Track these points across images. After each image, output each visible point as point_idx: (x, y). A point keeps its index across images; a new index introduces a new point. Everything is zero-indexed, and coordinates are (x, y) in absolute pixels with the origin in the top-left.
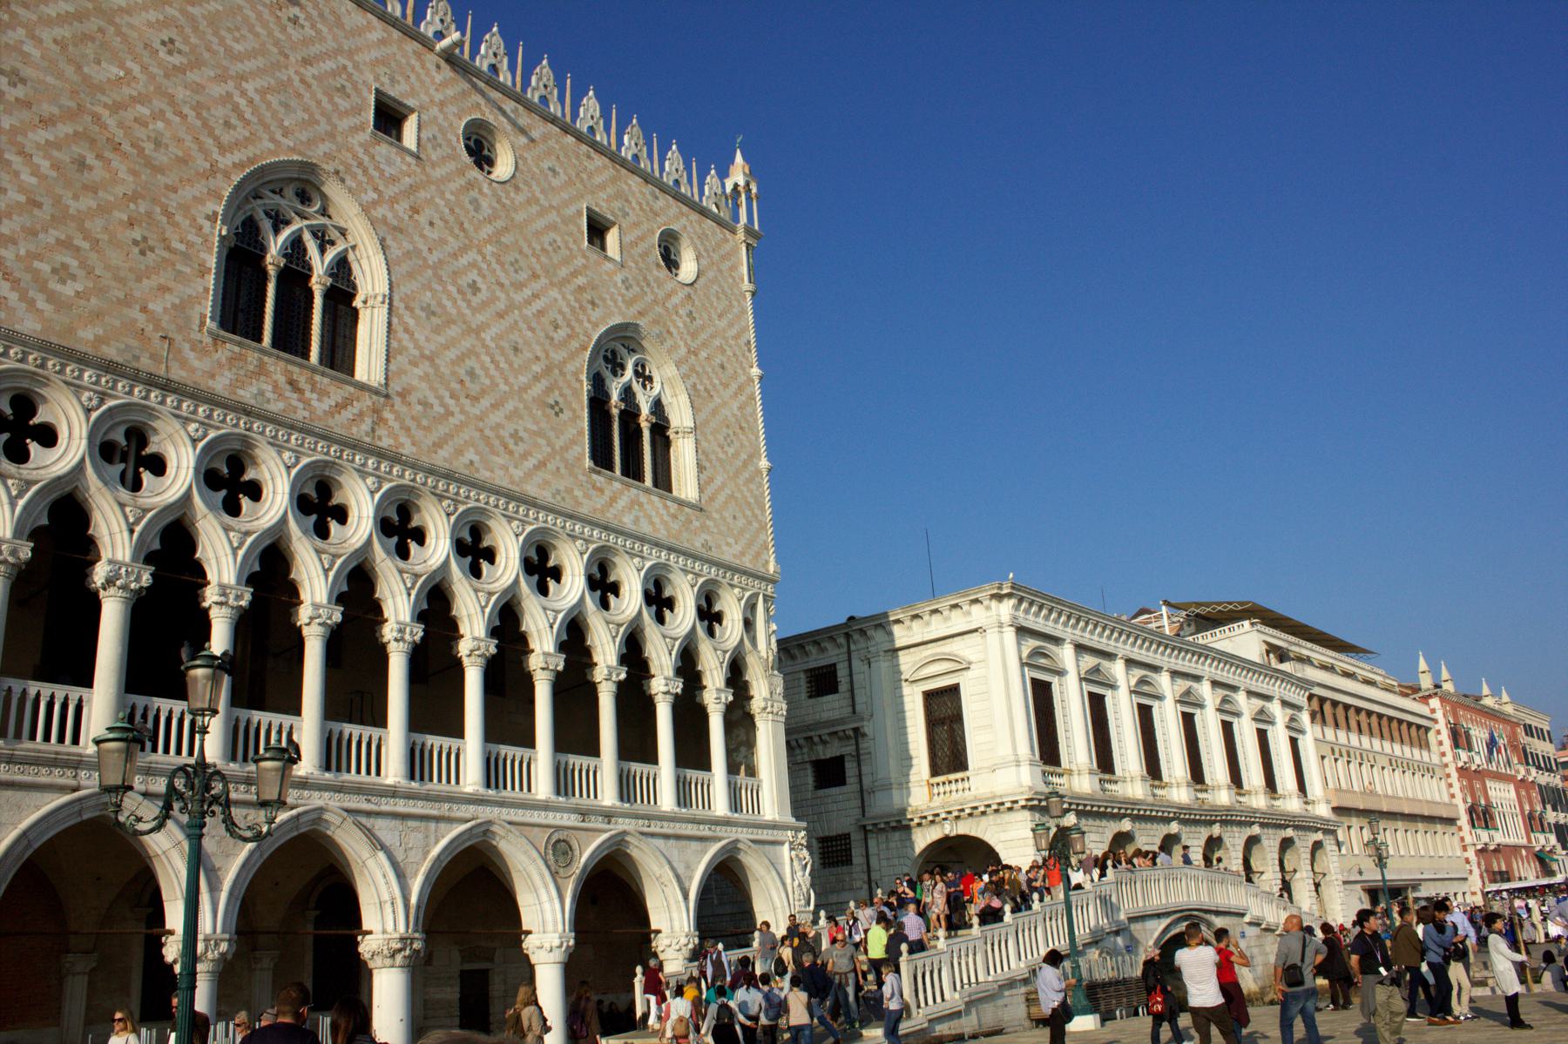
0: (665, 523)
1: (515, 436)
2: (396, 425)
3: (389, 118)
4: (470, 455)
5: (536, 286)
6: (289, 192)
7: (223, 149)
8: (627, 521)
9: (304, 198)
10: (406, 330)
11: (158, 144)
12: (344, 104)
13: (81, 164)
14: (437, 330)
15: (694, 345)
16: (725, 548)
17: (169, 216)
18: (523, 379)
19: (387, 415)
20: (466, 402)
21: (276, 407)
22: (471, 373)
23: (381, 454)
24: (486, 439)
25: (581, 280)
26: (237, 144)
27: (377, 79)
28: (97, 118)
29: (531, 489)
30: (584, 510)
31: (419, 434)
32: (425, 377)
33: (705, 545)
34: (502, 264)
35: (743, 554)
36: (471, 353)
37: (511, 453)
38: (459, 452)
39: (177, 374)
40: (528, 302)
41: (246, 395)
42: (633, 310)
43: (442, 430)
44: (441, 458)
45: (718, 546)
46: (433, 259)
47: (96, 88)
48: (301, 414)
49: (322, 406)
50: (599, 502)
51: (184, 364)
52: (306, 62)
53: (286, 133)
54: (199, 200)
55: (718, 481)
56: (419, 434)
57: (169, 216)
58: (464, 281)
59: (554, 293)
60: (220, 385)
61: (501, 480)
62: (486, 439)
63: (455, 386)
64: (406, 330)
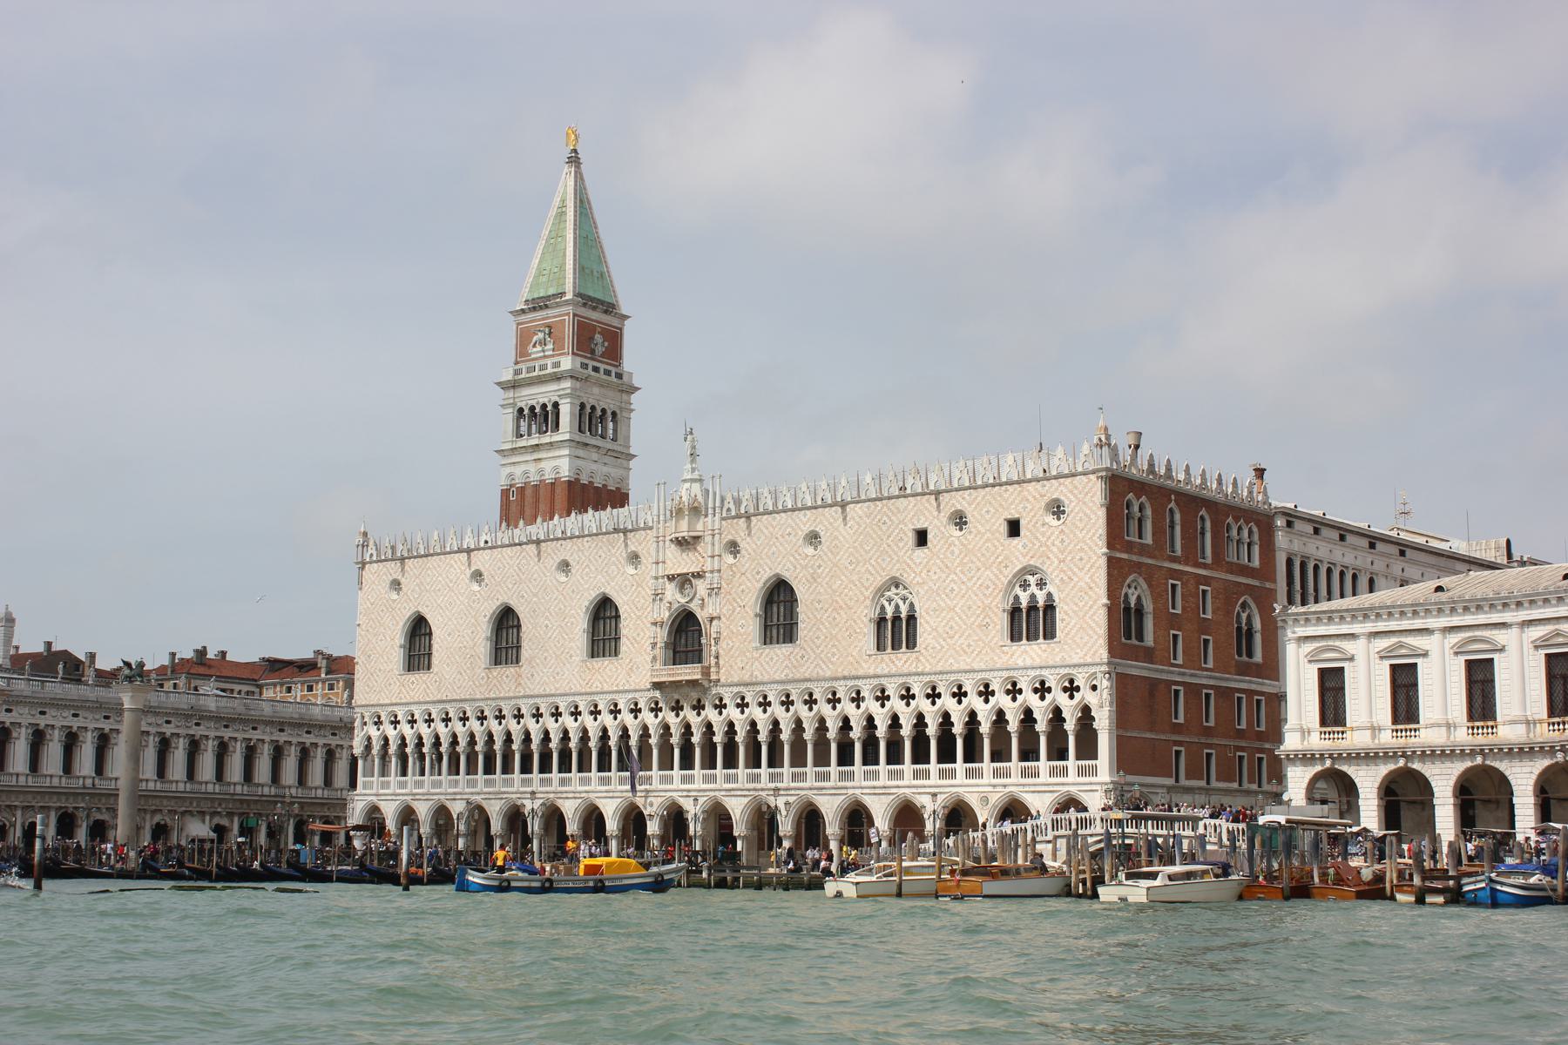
0: (1039, 656)
1: (969, 646)
2: (923, 660)
3: (922, 538)
4: (951, 661)
5: (979, 574)
6: (893, 588)
7: (867, 589)
8: (1020, 663)
9: (897, 587)
10: (927, 622)
11: (851, 599)
12: (901, 545)
13: (834, 619)
14: (937, 617)
15: (1062, 557)
16: (1074, 656)
17: (855, 621)
18: (973, 619)
19: (921, 658)
20: (948, 640)
21: (886, 672)
22: (951, 628)
23: (918, 674)
24: (957, 652)
25: (1000, 558)
26: (871, 584)
27: (913, 524)
28: (837, 602)
29: (976, 666)
30: (998, 666)
31: (931, 660)
32: (934, 638)
33: (1063, 659)
34: (963, 573)
35: (1086, 655)
36: (952, 618)
37: (965, 652)
38: (946, 661)
39: (861, 673)
40: (975, 584)
41: (879, 671)
42: (1028, 558)
43: (941, 655)
44: (939, 668)
45: (1070, 656)
46: (935, 588)
47: (834, 591)
48: (894, 671)
49: (899, 665)
50: (1005, 658)
51: (862, 667)
52: (889, 536)
53: (884, 570)
54: (862, 612)
55: (1073, 621)
56: (931, 660)
57: (855, 621)
58: (947, 591)
59: (988, 572)
60: (871, 672)
61: (963, 666)
62: (957, 652)
63: (945, 635)
64: (927, 622)
